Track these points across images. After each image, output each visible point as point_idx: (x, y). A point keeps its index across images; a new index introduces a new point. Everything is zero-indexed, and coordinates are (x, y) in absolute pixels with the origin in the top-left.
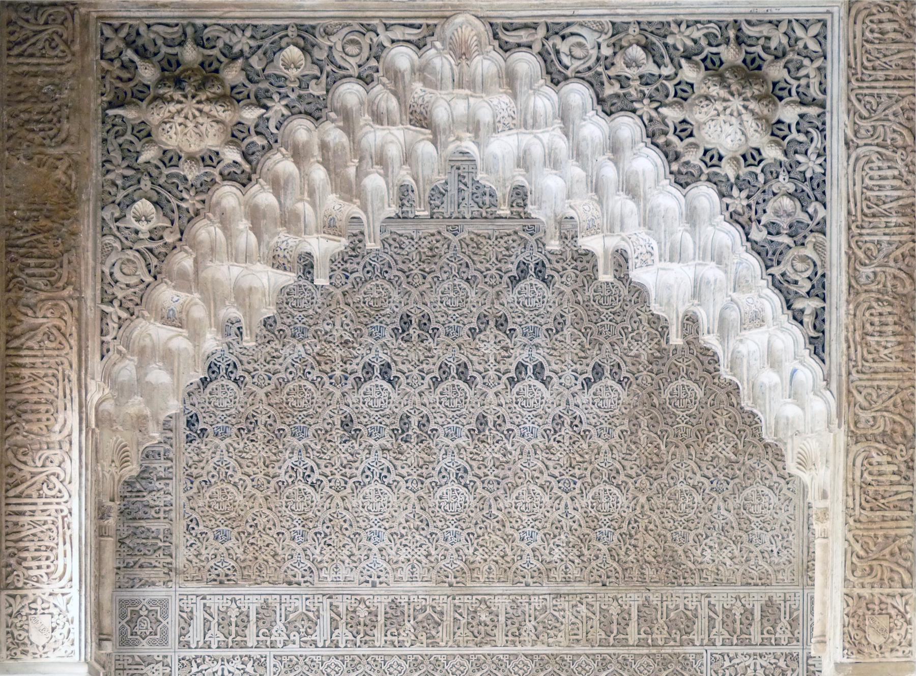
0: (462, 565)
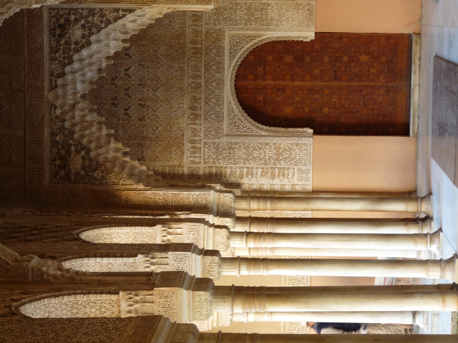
0: (179, 91)
